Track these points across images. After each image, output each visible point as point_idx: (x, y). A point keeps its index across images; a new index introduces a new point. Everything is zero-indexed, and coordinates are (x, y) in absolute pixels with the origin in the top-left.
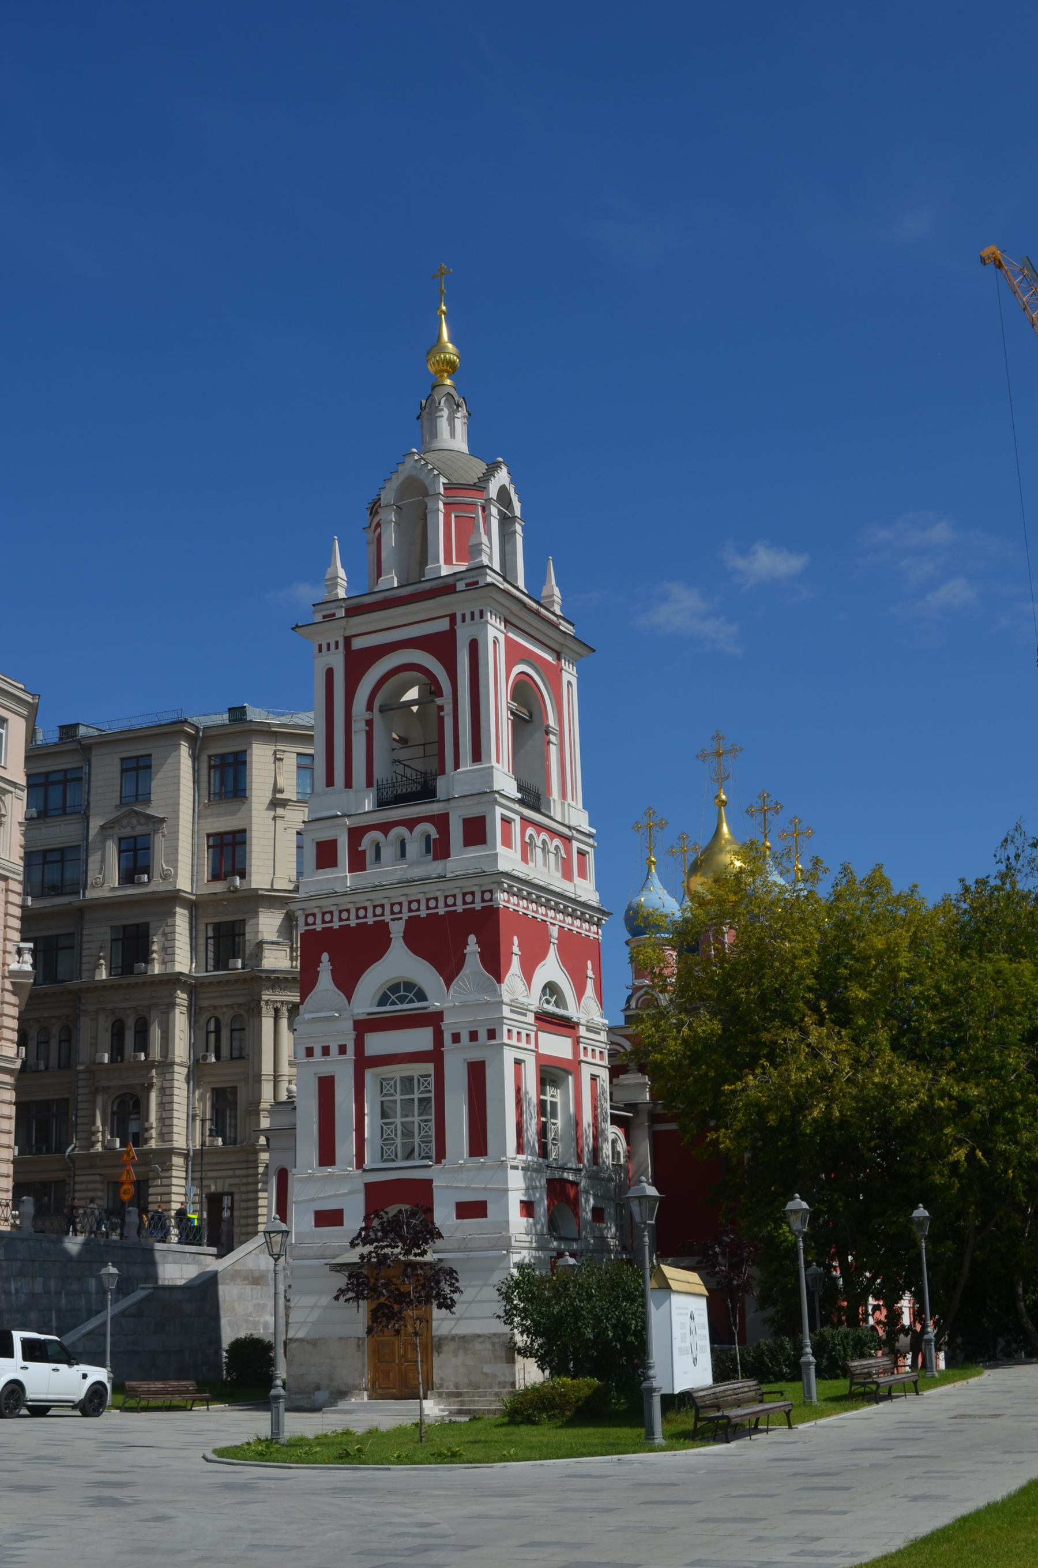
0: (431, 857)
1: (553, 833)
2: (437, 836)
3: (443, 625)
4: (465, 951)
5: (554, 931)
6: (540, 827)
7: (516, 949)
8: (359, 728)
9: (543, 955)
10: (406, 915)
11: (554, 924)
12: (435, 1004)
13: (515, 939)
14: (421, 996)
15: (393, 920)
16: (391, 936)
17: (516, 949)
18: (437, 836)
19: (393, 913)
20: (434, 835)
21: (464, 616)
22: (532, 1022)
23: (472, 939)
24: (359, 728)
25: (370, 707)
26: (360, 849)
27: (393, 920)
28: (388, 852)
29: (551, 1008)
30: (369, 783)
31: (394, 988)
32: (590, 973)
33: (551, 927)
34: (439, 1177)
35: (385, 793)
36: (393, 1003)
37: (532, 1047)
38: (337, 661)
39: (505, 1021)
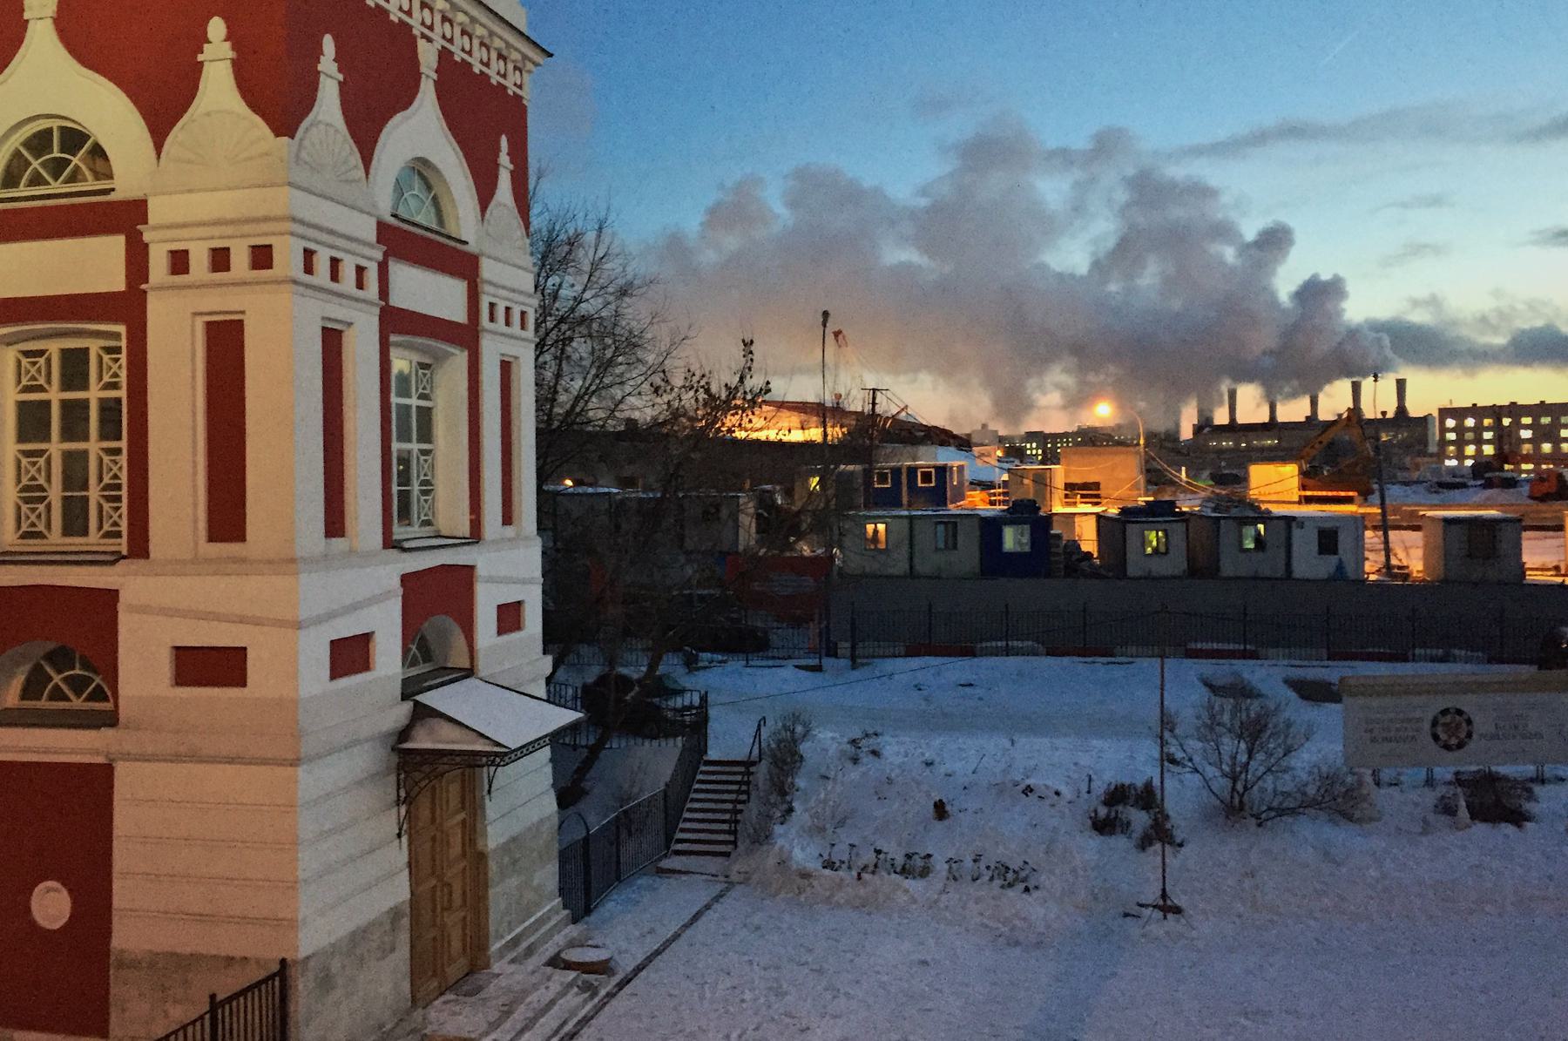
4: (200, 58)
5: (427, 56)
7: (328, 63)
9: (404, 97)
11: (429, 40)
12: (125, 185)
13: (328, 43)
16: (26, 16)
17: (328, 63)
22: (371, 235)
23: (217, 28)
31: (40, 142)
32: (504, 159)
33: (421, 43)
34: (130, 583)
36: (37, 180)
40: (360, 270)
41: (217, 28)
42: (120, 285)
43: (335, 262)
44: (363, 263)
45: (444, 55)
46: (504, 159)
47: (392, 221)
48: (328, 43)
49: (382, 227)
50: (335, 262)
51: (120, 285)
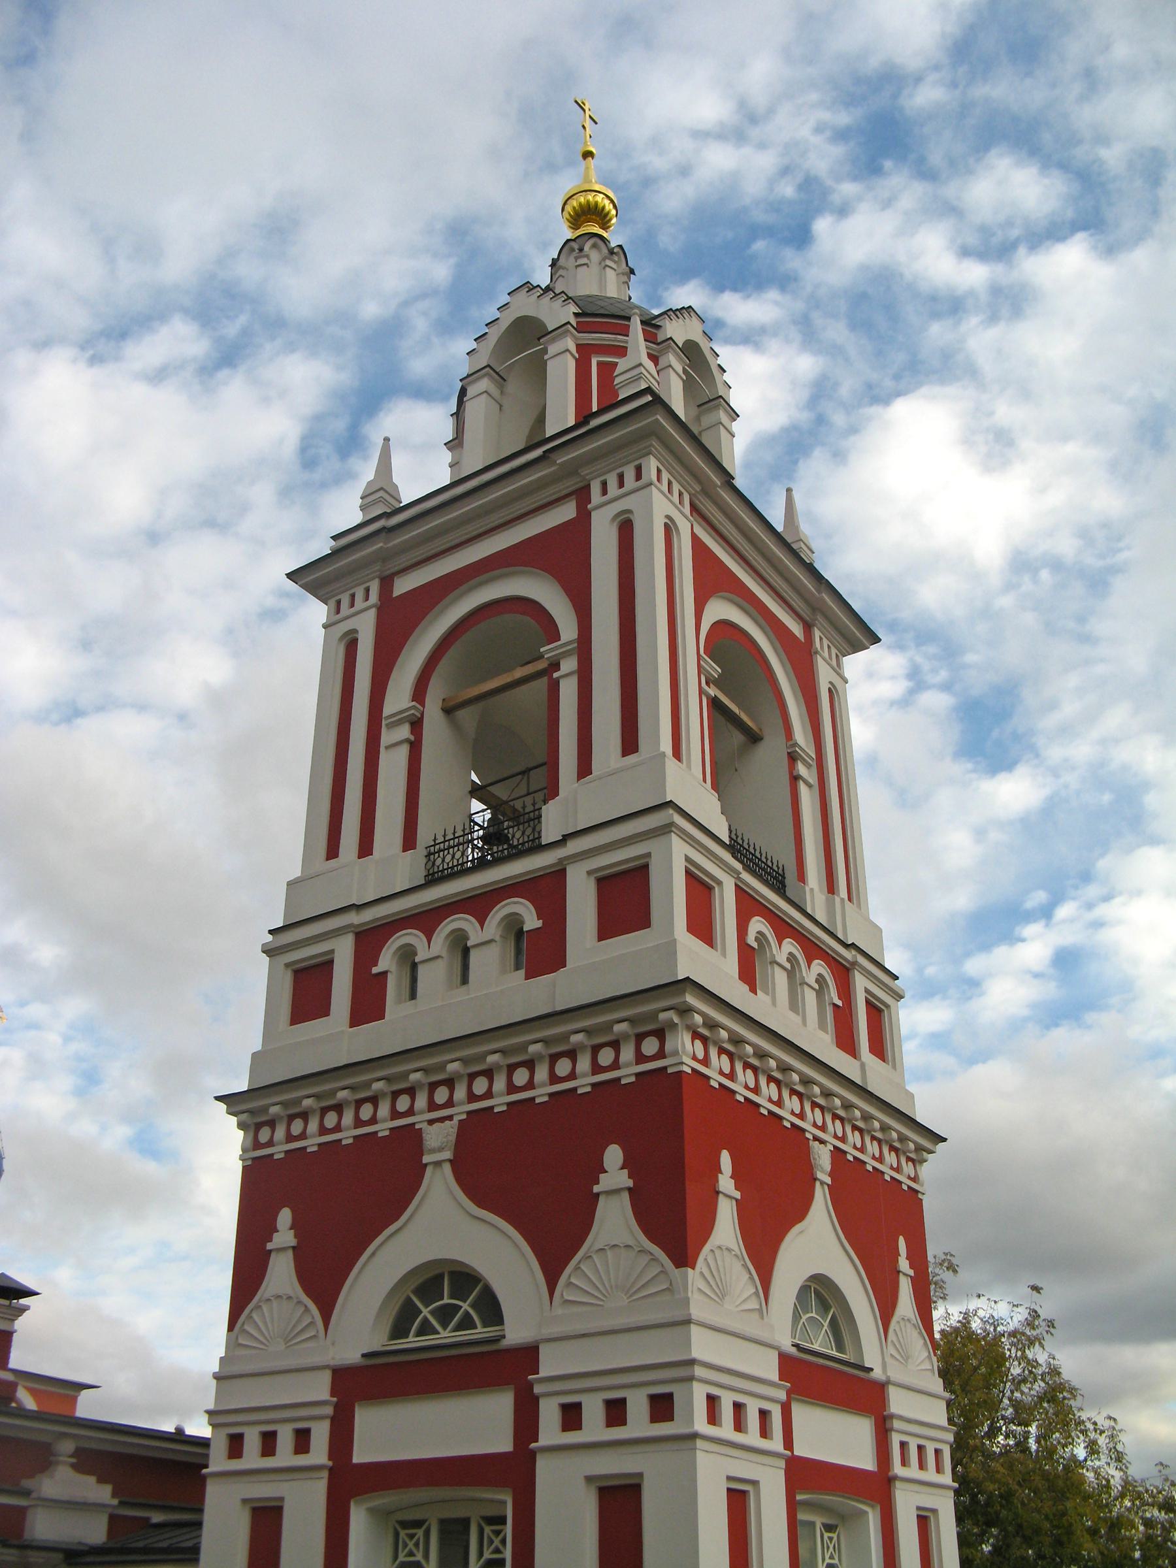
0: (522, 972)
1: (813, 950)
2: (539, 924)
3: (567, 512)
5: (822, 1158)
6: (783, 928)
7: (726, 1183)
8: (395, 735)
10: (461, 1111)
11: (822, 1142)
12: (515, 1333)
13: (725, 1159)
14: (491, 1309)
15: (431, 1122)
16: (426, 1159)
17: (726, 1183)
18: (539, 924)
19: (432, 1106)
20: (532, 922)
21: (604, 485)
22: (774, 1376)
23: (613, 1155)
24: (395, 735)
25: (419, 693)
26: (375, 970)
27: (431, 1122)
28: (433, 977)
29: (821, 1343)
30: (409, 842)
32: (904, 1264)
35: (439, 861)
36: (426, 1328)
37: (776, 1444)
38: (366, 626)
39: (699, 1371)
40: (764, 1414)
41: (613, 1155)
42: (504, 1444)
43: (738, 1407)
44: (766, 1406)
45: (838, 1153)
46: (904, 1264)
47: (793, 1350)
48: (725, 1159)
49: (784, 1358)
50: (738, 1407)
51: (504, 1444)
